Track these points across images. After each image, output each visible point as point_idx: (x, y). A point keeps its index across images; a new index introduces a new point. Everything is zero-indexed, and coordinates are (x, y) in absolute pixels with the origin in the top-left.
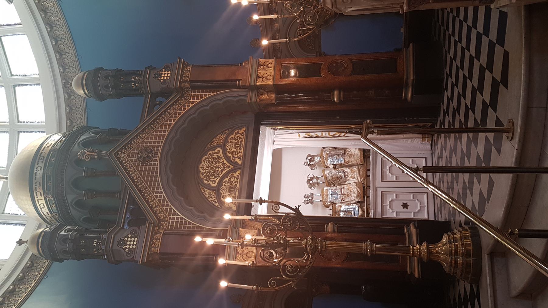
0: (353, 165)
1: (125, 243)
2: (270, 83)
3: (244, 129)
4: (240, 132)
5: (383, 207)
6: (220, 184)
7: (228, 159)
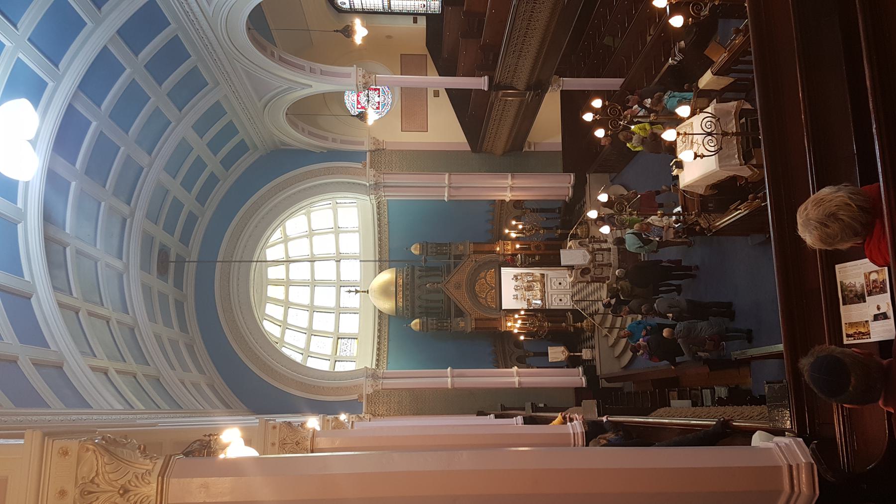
0: (538, 281)
1: (459, 324)
2: (510, 253)
3: (494, 270)
4: (493, 271)
5: (552, 301)
6: (486, 294)
7: (488, 284)
